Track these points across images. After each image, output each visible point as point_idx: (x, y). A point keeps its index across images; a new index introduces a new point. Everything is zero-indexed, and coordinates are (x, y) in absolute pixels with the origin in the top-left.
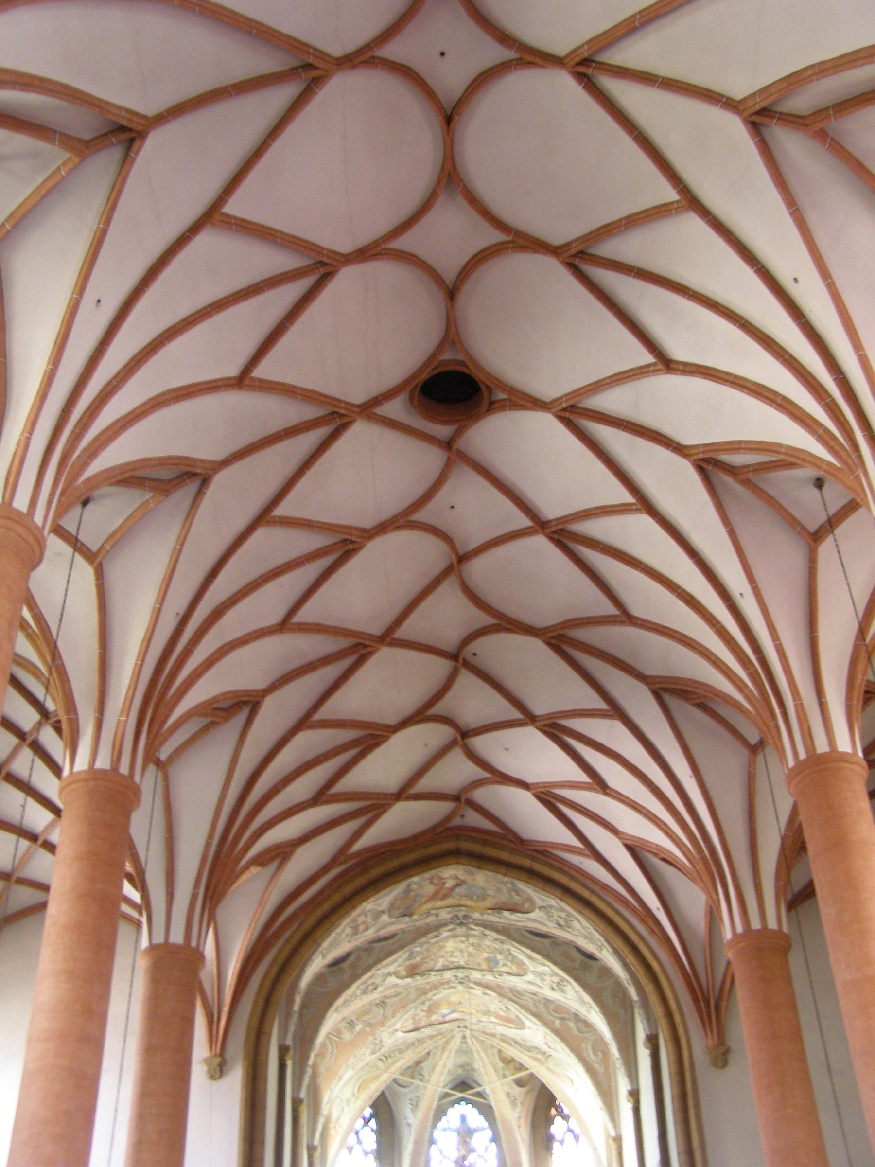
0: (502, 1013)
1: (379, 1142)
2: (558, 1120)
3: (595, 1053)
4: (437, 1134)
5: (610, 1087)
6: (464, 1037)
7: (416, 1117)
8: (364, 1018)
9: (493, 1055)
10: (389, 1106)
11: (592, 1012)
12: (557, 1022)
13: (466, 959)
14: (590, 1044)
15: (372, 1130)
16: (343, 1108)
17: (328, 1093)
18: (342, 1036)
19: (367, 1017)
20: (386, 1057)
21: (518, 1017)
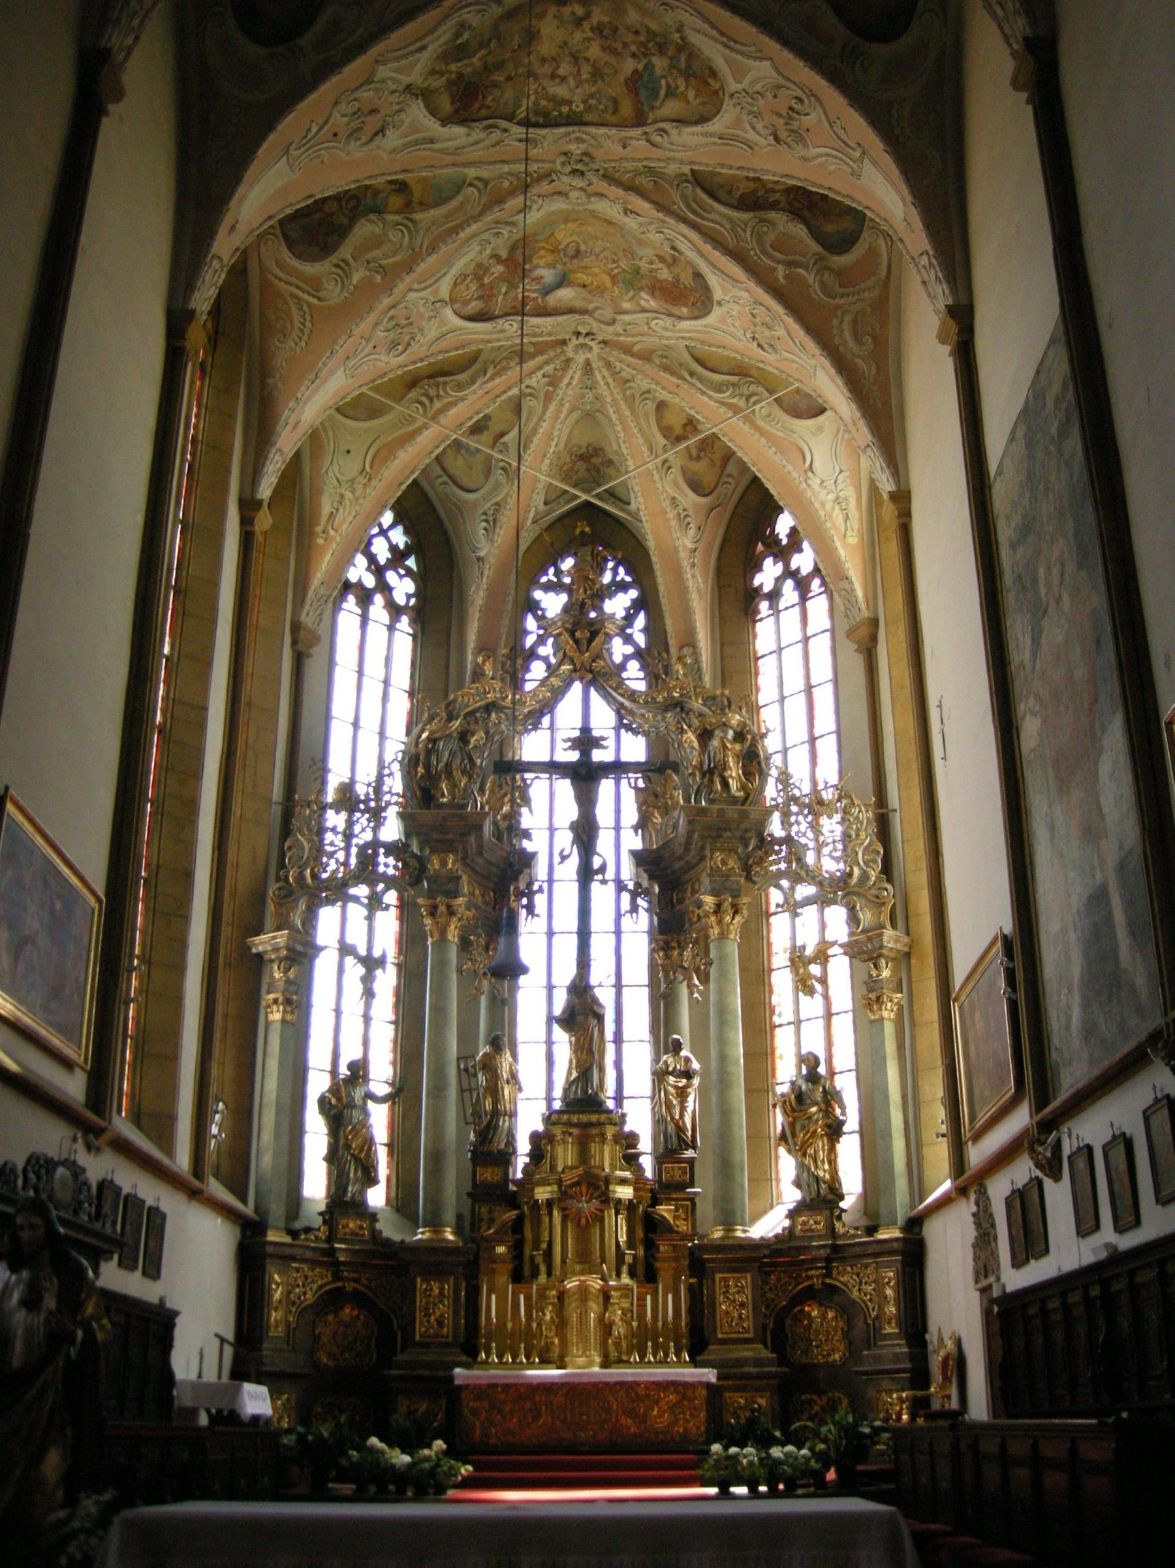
0: (665, 274)
1: (417, 594)
2: (768, 562)
3: (858, 339)
4: (538, 594)
5: (887, 405)
6: (588, 367)
7: (493, 541)
8: (369, 256)
9: (647, 415)
10: (445, 533)
11: (868, 169)
12: (781, 272)
13: (590, 89)
14: (847, 318)
15: (409, 572)
16: (342, 496)
17: (292, 404)
18: (322, 294)
19: (377, 253)
20: (431, 400)
21: (698, 275)
